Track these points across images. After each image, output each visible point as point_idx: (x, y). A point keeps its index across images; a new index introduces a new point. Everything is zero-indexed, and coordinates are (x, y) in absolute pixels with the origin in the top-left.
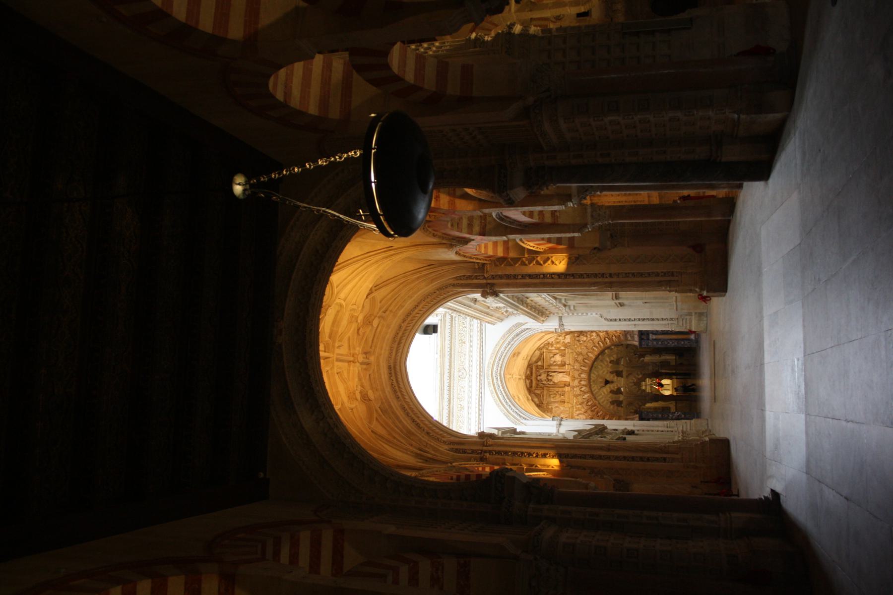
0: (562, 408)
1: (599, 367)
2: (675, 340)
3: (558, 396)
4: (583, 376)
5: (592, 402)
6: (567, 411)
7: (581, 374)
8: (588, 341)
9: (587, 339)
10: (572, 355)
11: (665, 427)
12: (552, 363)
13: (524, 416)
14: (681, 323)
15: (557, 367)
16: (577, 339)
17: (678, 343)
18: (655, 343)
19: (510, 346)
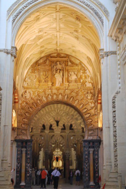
0: (35, 81)
1: (68, 117)
2: (89, 170)
3: (44, 77)
4: (60, 96)
5: (39, 103)
6: (33, 84)
7: (62, 95)
8: (87, 101)
9: (89, 99)
10: (76, 88)
11: (3, 158)
12: (70, 73)
13: (17, 20)
14: (111, 175)
15: (66, 76)
16: (89, 92)
17: (87, 171)
18: (86, 153)
19: (85, 6)
